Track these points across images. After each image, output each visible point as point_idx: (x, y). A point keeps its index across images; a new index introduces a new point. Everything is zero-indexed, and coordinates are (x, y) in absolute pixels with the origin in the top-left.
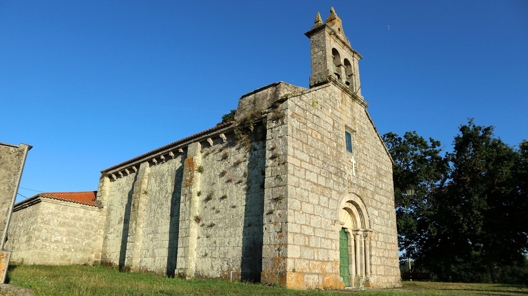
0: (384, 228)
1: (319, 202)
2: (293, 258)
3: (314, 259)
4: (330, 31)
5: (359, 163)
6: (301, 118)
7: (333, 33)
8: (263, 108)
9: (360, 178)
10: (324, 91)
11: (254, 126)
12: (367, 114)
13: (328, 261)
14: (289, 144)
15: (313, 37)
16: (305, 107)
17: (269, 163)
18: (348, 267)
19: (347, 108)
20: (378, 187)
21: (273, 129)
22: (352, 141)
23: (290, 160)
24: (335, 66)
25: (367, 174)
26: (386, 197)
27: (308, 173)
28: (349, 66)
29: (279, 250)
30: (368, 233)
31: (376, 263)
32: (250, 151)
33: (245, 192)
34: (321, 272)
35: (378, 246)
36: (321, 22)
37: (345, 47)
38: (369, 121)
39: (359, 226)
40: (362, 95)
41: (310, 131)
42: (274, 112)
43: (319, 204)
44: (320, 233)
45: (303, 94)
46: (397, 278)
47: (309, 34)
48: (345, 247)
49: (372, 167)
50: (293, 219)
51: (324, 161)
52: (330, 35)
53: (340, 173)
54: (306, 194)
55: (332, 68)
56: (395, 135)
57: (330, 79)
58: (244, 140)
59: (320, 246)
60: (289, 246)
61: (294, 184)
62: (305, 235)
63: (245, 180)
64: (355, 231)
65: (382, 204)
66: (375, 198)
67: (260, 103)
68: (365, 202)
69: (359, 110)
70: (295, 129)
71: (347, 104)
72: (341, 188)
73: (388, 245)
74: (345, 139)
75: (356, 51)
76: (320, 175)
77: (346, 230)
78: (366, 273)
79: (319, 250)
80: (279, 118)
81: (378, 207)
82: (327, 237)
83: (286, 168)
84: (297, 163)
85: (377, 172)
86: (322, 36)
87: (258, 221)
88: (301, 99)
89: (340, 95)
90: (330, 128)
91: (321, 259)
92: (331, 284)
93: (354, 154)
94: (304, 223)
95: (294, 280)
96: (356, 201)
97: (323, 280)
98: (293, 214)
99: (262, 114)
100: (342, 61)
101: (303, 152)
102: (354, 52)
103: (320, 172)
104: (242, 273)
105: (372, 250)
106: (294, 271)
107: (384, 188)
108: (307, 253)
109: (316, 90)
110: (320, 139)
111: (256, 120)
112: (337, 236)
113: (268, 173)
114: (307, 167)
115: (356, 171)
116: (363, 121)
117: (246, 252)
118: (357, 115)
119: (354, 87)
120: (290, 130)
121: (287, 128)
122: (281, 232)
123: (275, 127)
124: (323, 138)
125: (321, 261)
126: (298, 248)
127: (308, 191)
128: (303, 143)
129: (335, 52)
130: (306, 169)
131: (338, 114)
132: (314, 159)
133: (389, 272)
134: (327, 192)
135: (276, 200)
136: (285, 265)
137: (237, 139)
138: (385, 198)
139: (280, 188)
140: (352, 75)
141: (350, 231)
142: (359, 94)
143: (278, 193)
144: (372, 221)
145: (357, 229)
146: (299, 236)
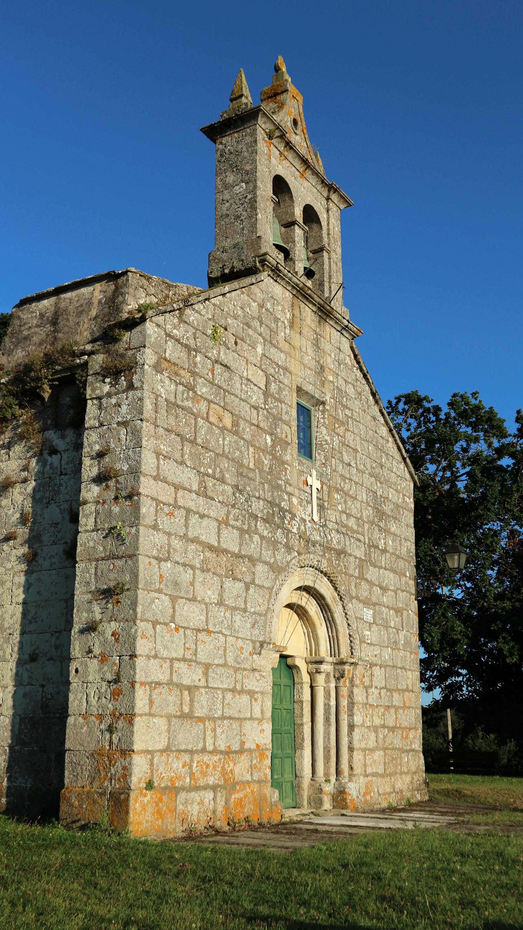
0: (387, 653)
1: (221, 595)
2: (147, 752)
3: (204, 750)
4: (269, 127)
5: (329, 487)
6: (182, 372)
7: (277, 134)
8: (78, 338)
9: (330, 525)
10: (244, 297)
11: (51, 387)
12: (355, 356)
13: (241, 751)
14: (144, 443)
15: (224, 140)
16: (192, 343)
17: (91, 492)
18: (292, 758)
19: (304, 342)
20: (376, 547)
21: (104, 401)
22: (314, 429)
23: (147, 487)
24: (277, 226)
25: (349, 515)
26: (394, 571)
27: (194, 519)
28: (315, 226)
29: (111, 730)
30: (347, 667)
31: (363, 745)
32: (40, 455)
33: (24, 567)
34: (222, 782)
35: (370, 701)
36: (248, 100)
37: (308, 173)
38: (359, 374)
40: (346, 303)
41: (203, 406)
42: (108, 352)
43: (220, 603)
44: (221, 680)
45: (187, 303)
46: (416, 778)
47: (214, 132)
48: (287, 705)
49: (363, 496)
50: (151, 645)
51: (236, 487)
52: (270, 137)
53: (278, 515)
54: (187, 576)
55: (269, 232)
56: (426, 398)
57: (263, 262)
58: (25, 423)
59: (220, 713)
60: (137, 719)
61: (155, 553)
62: (181, 687)
63: (23, 532)
64: (312, 663)
65: (384, 589)
66: (368, 577)
67: (71, 323)
68: (342, 589)
69: (336, 344)
70: (162, 403)
71: (305, 330)
72: (281, 556)
73: (395, 695)
74: (294, 424)
75: (336, 185)
76: (227, 524)
77: (289, 661)
78: (338, 772)
79: (219, 722)
80: (121, 371)
81: (374, 599)
82: (238, 687)
83: (136, 508)
84: (166, 494)
85: (374, 508)
86: (248, 139)
87: (57, 647)
88: (180, 318)
89: (287, 305)
90: (257, 398)
91: (223, 748)
92: (248, 810)
93: (318, 463)
94: (179, 654)
95: (150, 810)
96: (317, 587)
97: (227, 801)
98: (152, 632)
99: (74, 355)
100: (298, 213)
101: (182, 463)
102: (331, 188)
103: (229, 512)
104: (9, 788)
105: (355, 710)
106: (150, 785)
107: (390, 549)
108: (187, 736)
109: (224, 295)
110: (229, 425)
111: (57, 372)
112: (264, 683)
113: (87, 520)
114: (191, 505)
115: (321, 507)
116: (343, 374)
117: (20, 731)
118: (329, 360)
119: (326, 284)
120: (148, 405)
121: (141, 399)
122: (117, 681)
123: (109, 395)
124: (238, 425)
125: (221, 752)
126: (161, 723)
127: (193, 567)
128: (183, 438)
129: (280, 186)
130: (188, 511)
131: (280, 358)
132: (210, 483)
133: (396, 766)
134: (243, 568)
135: (108, 594)
136: (127, 772)
137: (4, 420)
138: (392, 575)
139: (119, 563)
140: (321, 249)
141: (300, 663)
142: (338, 305)
143: (112, 576)
144: (356, 636)
145: (318, 659)
146: (164, 690)
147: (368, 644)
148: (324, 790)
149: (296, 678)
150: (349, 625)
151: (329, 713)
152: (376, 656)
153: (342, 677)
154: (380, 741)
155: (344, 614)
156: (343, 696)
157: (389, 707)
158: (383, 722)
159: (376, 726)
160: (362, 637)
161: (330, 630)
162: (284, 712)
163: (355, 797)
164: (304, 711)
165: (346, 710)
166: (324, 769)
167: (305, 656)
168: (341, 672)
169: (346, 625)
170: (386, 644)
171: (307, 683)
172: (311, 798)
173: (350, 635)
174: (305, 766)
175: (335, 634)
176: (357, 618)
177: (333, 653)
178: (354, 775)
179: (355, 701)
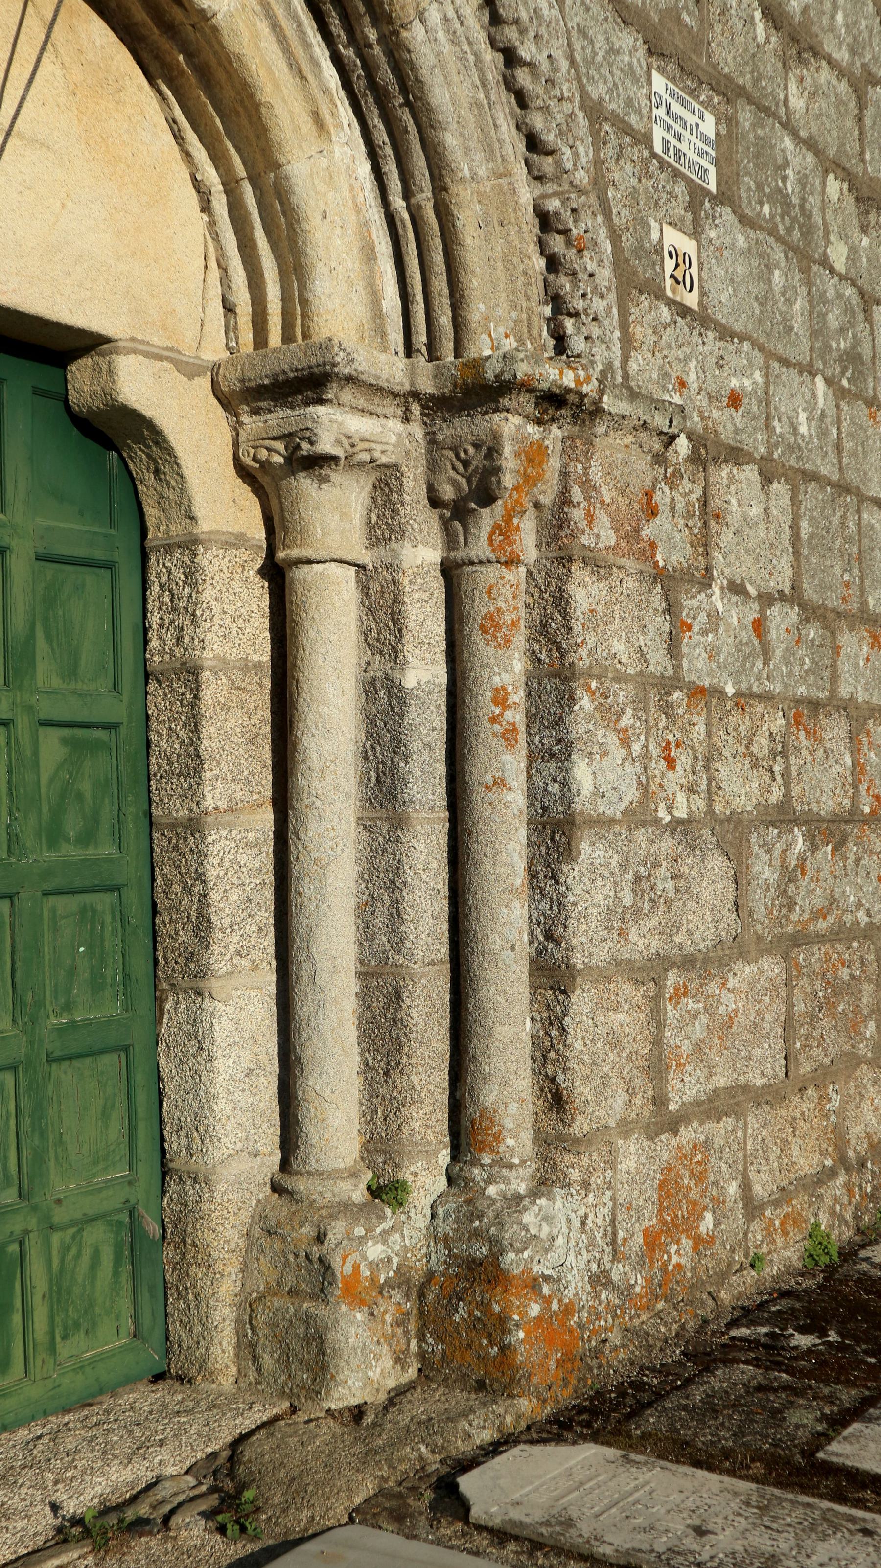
30: (513, 426)
31: (642, 941)
35: (697, 665)
39: (351, 297)
78: (465, 1132)
144: (590, 225)
147: (684, 311)
148: (342, 1268)
149: (152, 513)
150: (533, 143)
151: (397, 745)
152: (735, 400)
153: (487, 498)
154: (760, 902)
155: (492, 59)
156: (490, 626)
157: (815, 705)
158: (776, 794)
159: (734, 819)
161: (391, 169)
162: (52, 747)
163: (576, 1286)
164: (208, 730)
165: (516, 717)
166: (369, 1115)
167: (214, 351)
169: (513, 146)
170: (801, 351)
171: (236, 541)
172: (261, 1318)
173: (546, 221)
174: (222, 1106)
175: (425, 198)
176: (595, 112)
177: (421, 338)
178: (575, 1144)
179: (582, 658)
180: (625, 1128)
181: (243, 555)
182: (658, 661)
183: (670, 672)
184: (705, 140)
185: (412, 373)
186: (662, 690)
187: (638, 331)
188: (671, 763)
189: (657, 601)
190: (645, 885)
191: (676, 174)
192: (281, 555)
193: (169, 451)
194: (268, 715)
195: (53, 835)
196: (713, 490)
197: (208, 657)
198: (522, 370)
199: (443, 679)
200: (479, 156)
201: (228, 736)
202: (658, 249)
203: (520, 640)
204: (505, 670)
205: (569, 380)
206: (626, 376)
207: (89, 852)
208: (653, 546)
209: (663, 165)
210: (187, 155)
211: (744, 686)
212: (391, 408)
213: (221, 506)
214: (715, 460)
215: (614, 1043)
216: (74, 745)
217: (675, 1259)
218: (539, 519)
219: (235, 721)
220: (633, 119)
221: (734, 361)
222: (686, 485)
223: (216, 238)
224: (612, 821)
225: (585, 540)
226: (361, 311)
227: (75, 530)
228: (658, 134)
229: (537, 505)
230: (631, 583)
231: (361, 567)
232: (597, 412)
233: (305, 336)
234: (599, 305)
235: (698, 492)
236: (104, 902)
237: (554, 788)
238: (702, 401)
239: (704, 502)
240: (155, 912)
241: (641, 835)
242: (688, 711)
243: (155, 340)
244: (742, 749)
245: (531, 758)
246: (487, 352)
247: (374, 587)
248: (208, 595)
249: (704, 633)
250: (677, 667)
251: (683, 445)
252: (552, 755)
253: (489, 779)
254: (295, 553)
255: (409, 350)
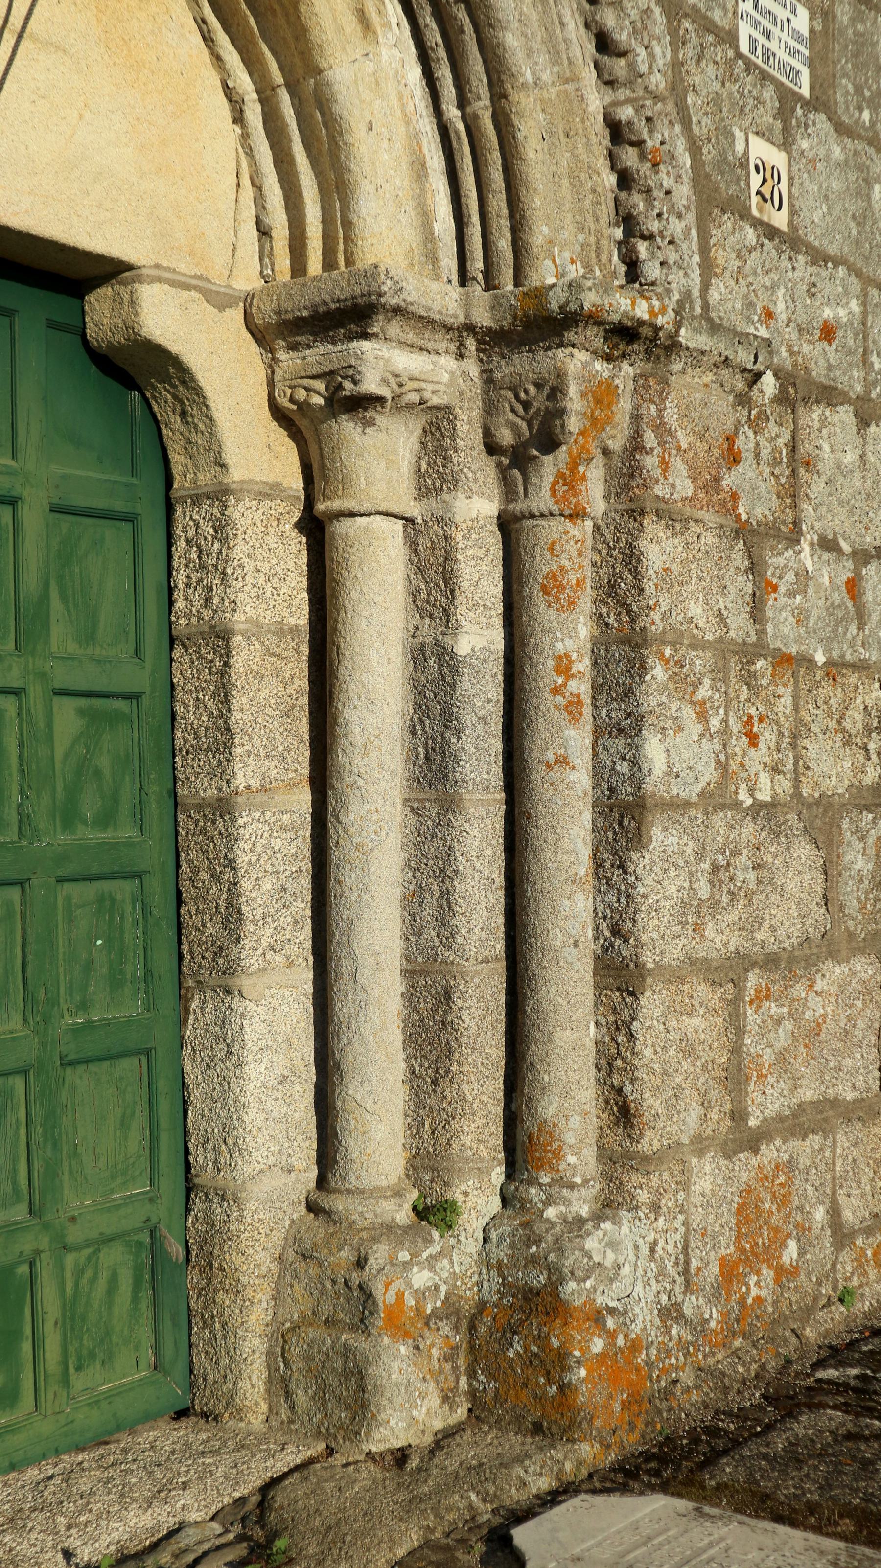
30: (579, 363)
31: (720, 938)
35: (783, 630)
39: (400, 216)
78: (521, 1147)
147: (771, 232)
148: (385, 1297)
149: (178, 460)
150: (604, 43)
151: (449, 718)
152: (828, 333)
153: (549, 442)
156: (553, 586)
159: (824, 803)
160: (722, 162)
162: (67, 718)
163: (644, 1319)
164: (239, 700)
165: (581, 687)
166: (415, 1128)
167: (247, 279)
168: (539, 402)
169: (582, 47)
171: (271, 492)
172: (295, 1351)
173: (617, 132)
174: (252, 1116)
175: (482, 107)
177: (477, 264)
178: (644, 1163)
179: (655, 622)
180: (700, 1145)
181: (279, 506)
182: (740, 626)
183: (753, 638)
184: (798, 38)
185: (467, 303)
186: (744, 657)
187: (720, 256)
188: (753, 740)
189: (739, 559)
190: (724, 876)
191: (765, 77)
192: (320, 507)
193: (198, 391)
194: (305, 684)
195: (69, 817)
196: (802, 434)
197: (239, 620)
198: (590, 300)
199: (500, 645)
200: (543, 59)
201: (261, 708)
202: (744, 163)
203: (586, 602)
204: (569, 635)
205: (642, 311)
206: (706, 306)
207: (108, 835)
208: (735, 497)
209: (750, 66)
210: (218, 59)
211: (835, 654)
212: (443, 342)
213: (253, 451)
214: (805, 400)
215: (688, 1050)
216: (92, 717)
217: (754, 1292)
218: (608, 467)
219: (269, 690)
220: (717, 15)
221: (828, 289)
222: (772, 428)
223: (250, 152)
224: (687, 804)
225: (658, 491)
226: (411, 235)
227: (93, 478)
228: (745, 31)
229: (606, 452)
230: (710, 539)
231: (409, 521)
232: (673, 346)
233: (349, 262)
234: (676, 227)
235: (786, 437)
236: (124, 889)
237: (623, 767)
238: (791, 333)
239: (793, 448)
240: (180, 902)
241: (719, 820)
242: (773, 682)
243: (182, 267)
244: (833, 724)
245: (597, 734)
246: (551, 280)
247: (424, 543)
248: (240, 551)
249: (792, 594)
250: (761, 633)
251: (769, 384)
252: (621, 730)
253: (550, 756)
254: (336, 505)
255: (464, 278)
